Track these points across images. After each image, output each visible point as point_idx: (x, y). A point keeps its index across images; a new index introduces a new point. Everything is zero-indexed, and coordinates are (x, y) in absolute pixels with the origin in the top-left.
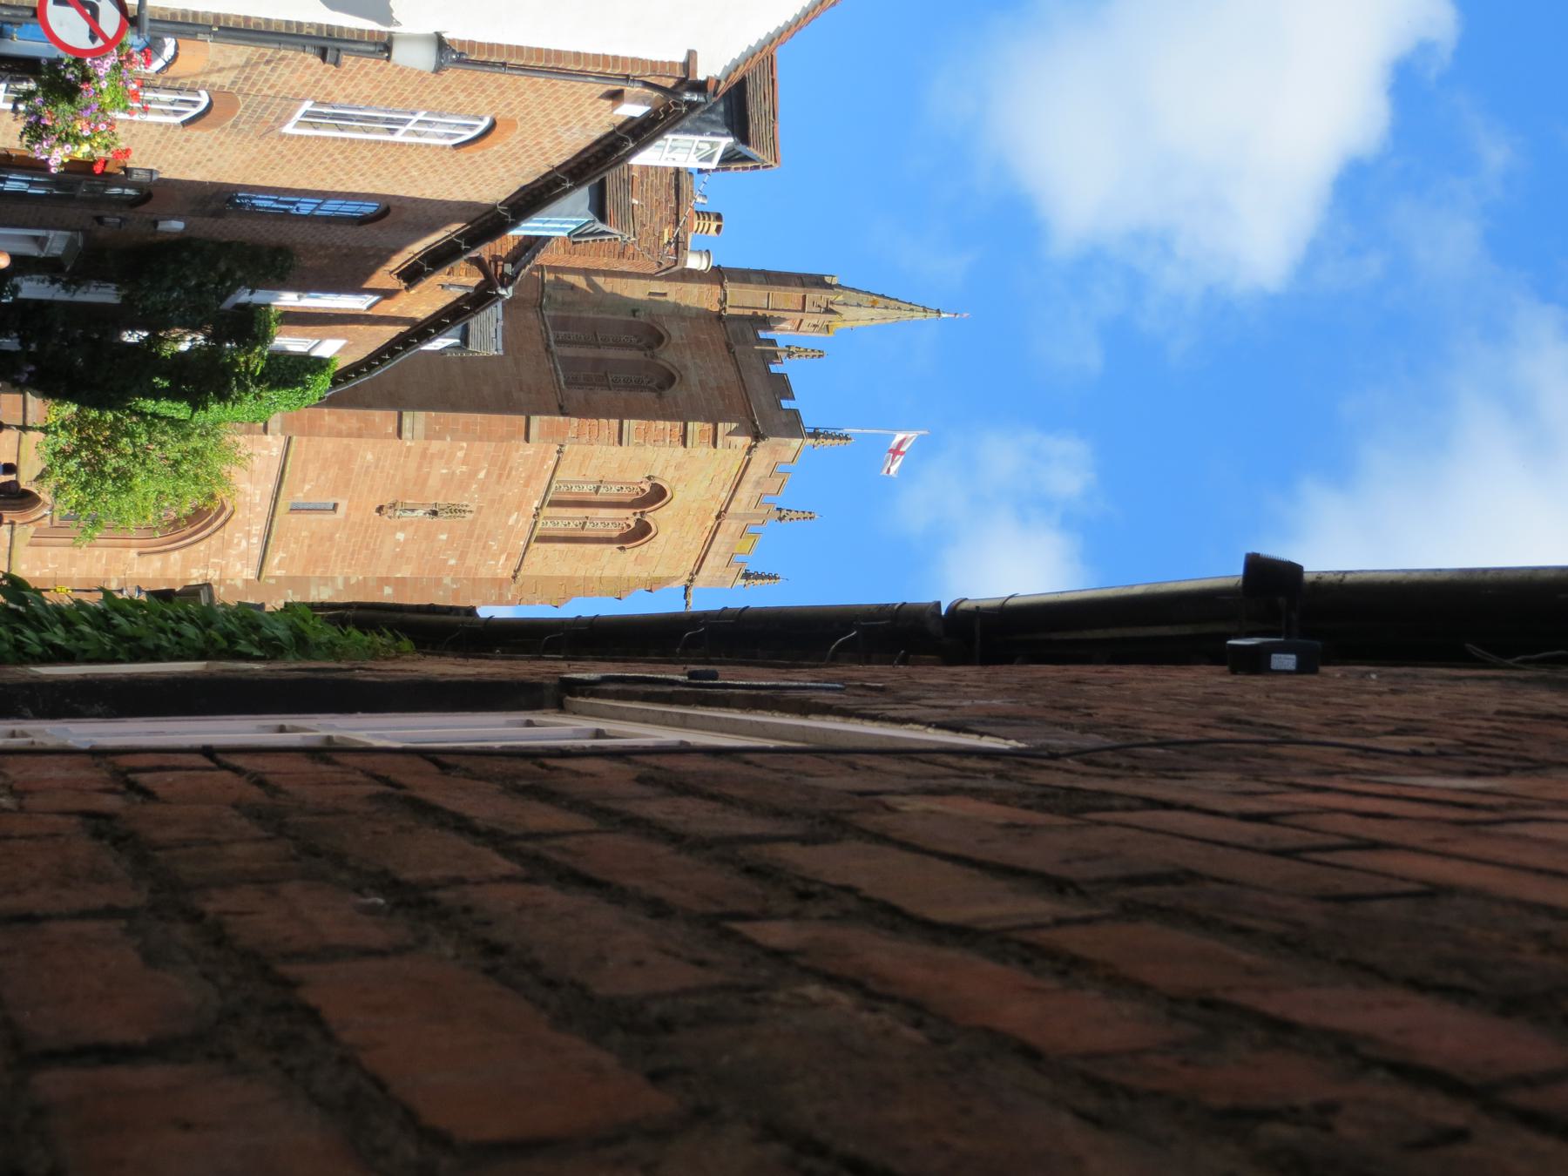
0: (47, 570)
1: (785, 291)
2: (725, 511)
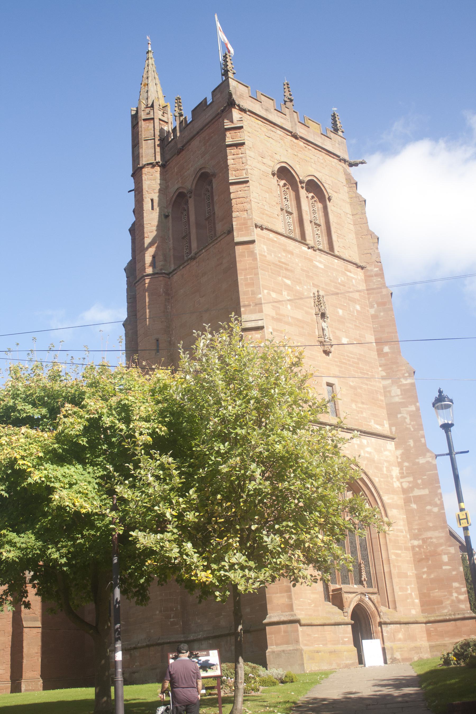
0: (413, 593)
1: (142, 131)
2: (291, 132)
